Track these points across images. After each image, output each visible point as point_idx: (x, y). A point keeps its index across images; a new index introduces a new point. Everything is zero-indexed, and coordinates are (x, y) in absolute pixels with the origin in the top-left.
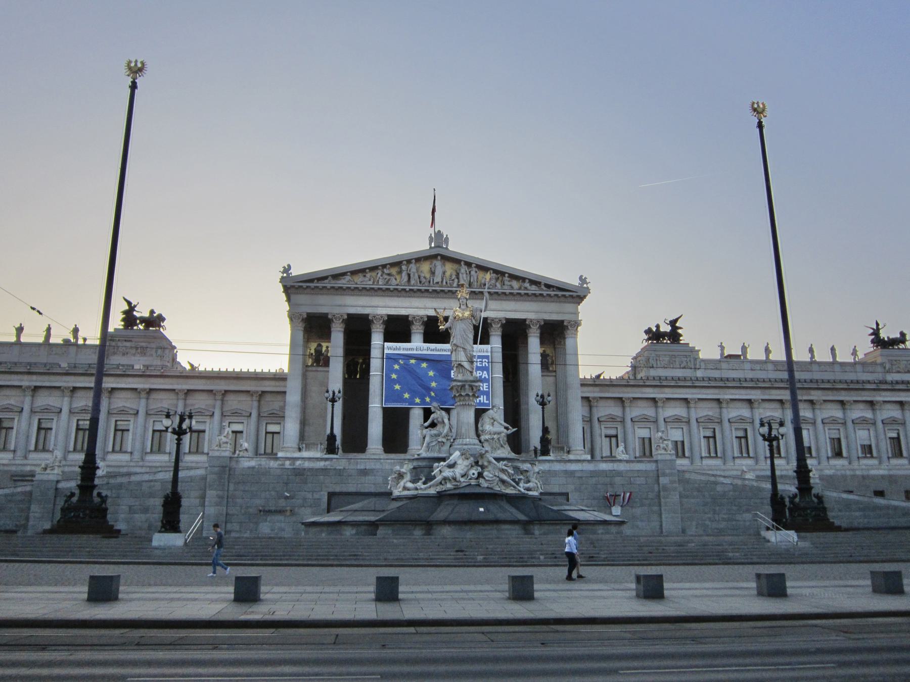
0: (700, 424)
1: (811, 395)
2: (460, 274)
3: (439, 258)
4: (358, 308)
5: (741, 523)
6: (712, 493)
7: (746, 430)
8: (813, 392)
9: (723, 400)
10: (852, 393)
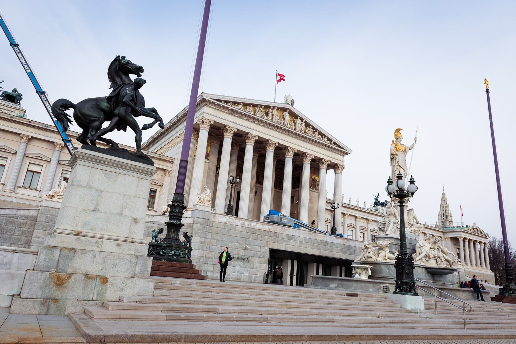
2: (297, 124)
3: (288, 111)
4: (243, 127)
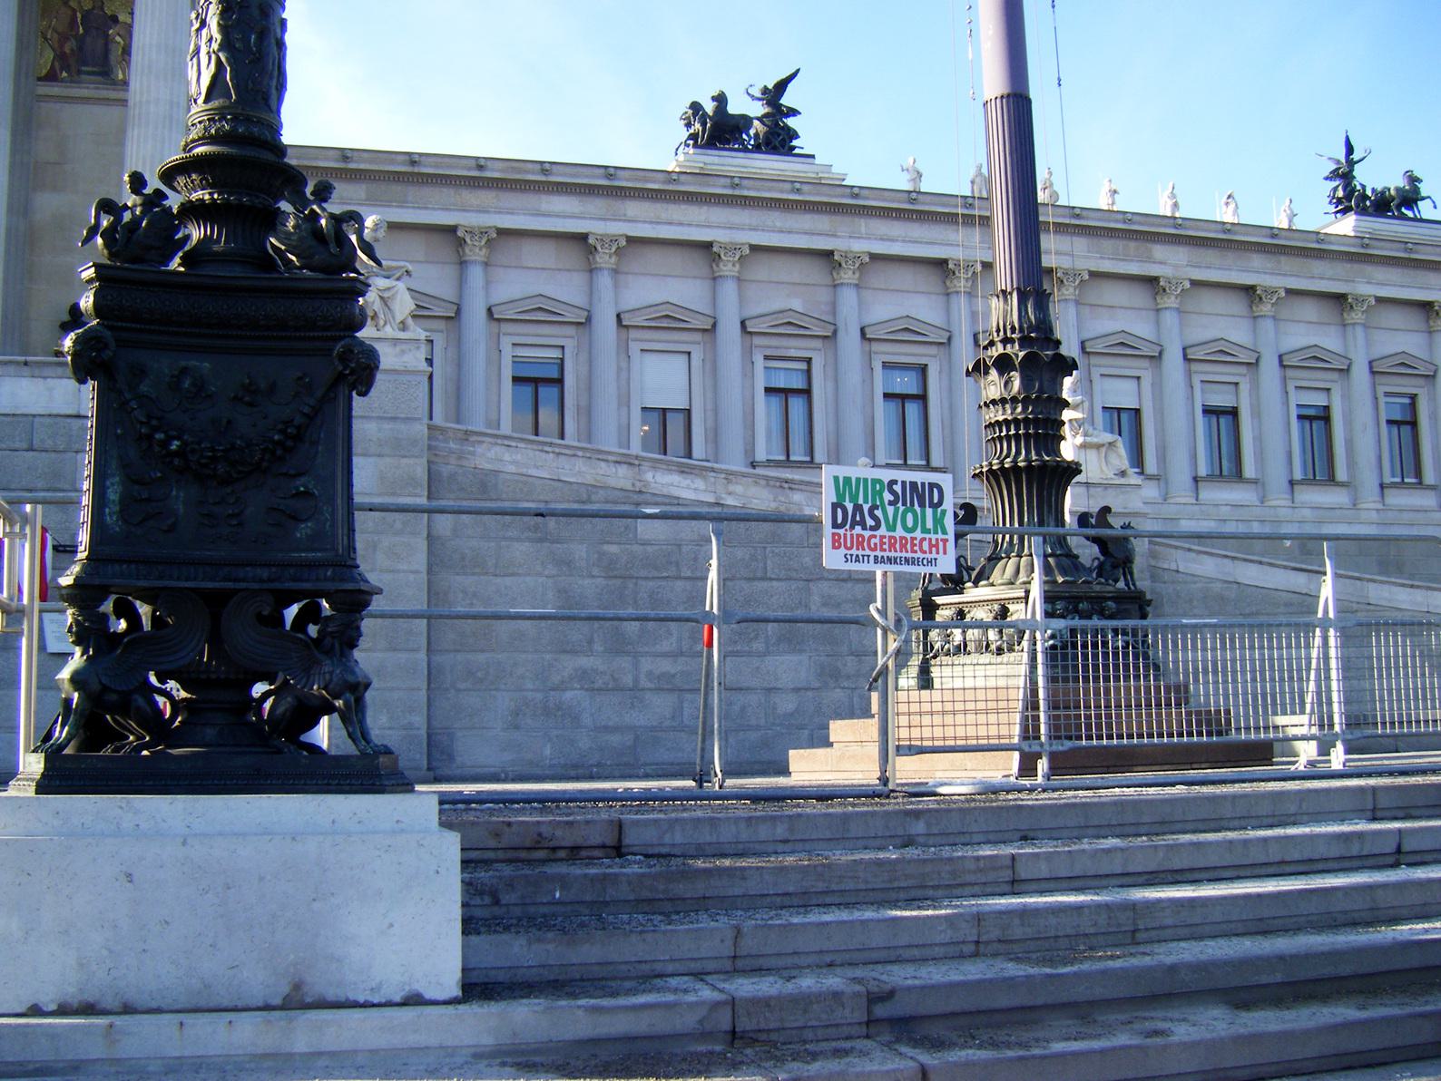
0: (757, 341)
1: (1150, 260)
5: (753, 699)
6: (613, 549)
7: (923, 370)
8: (1159, 251)
9: (845, 255)
10: (1287, 263)
